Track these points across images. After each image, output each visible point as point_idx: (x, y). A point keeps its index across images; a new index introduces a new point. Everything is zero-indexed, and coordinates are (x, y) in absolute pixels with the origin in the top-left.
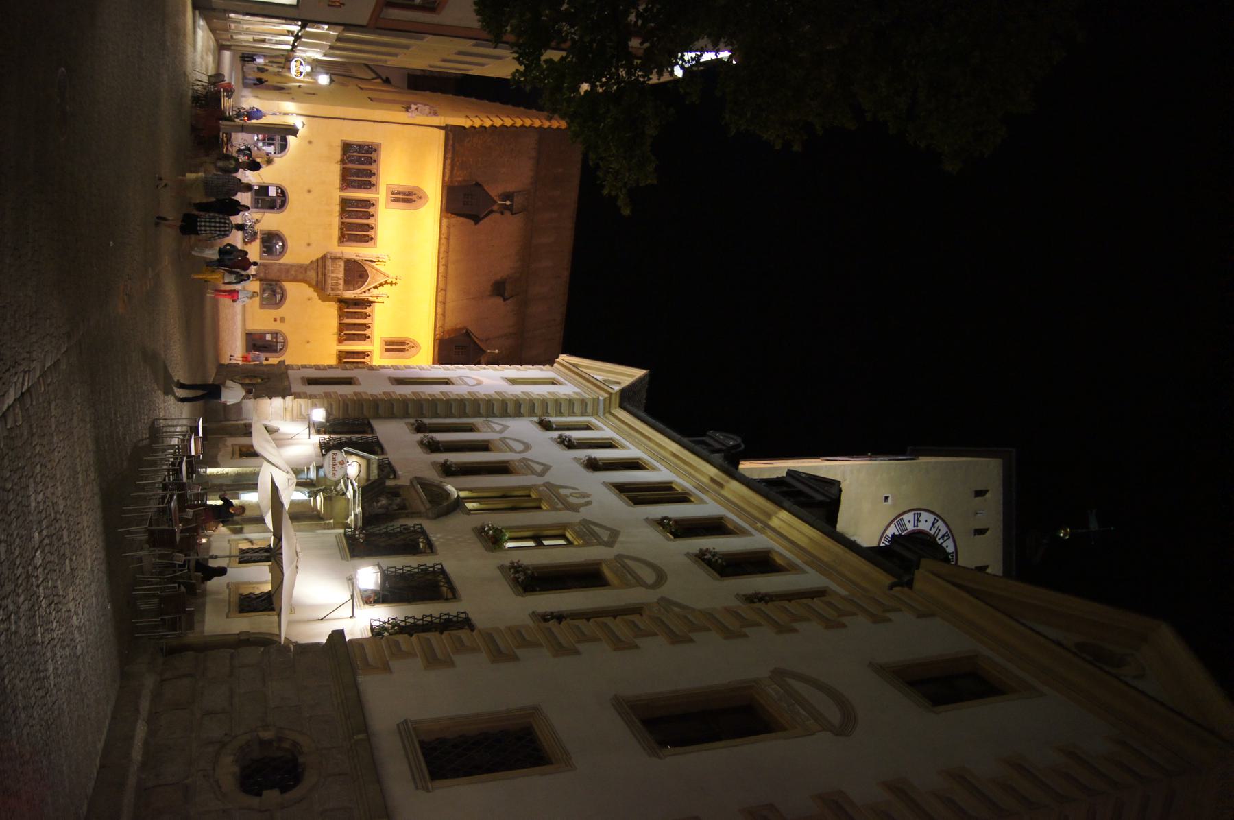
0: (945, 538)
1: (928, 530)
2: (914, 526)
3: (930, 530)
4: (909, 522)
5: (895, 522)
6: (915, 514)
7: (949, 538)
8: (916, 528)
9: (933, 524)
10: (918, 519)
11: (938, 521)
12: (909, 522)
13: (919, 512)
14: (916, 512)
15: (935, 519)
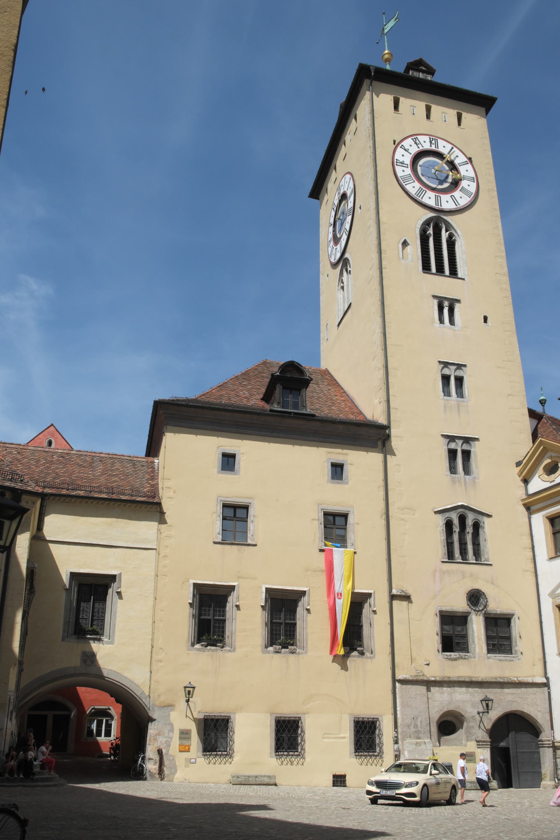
0: (417, 141)
1: (411, 155)
2: (408, 167)
3: (411, 154)
4: (403, 171)
5: (404, 184)
6: (397, 165)
7: (417, 138)
8: (409, 166)
9: (406, 150)
10: (402, 163)
11: (402, 145)
12: (403, 171)
13: (395, 161)
14: (395, 163)
15: (401, 147)
